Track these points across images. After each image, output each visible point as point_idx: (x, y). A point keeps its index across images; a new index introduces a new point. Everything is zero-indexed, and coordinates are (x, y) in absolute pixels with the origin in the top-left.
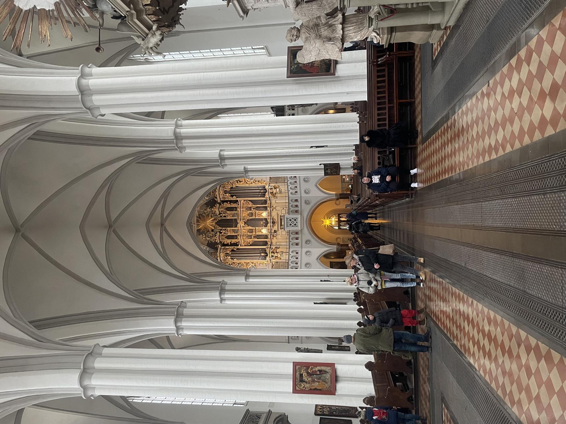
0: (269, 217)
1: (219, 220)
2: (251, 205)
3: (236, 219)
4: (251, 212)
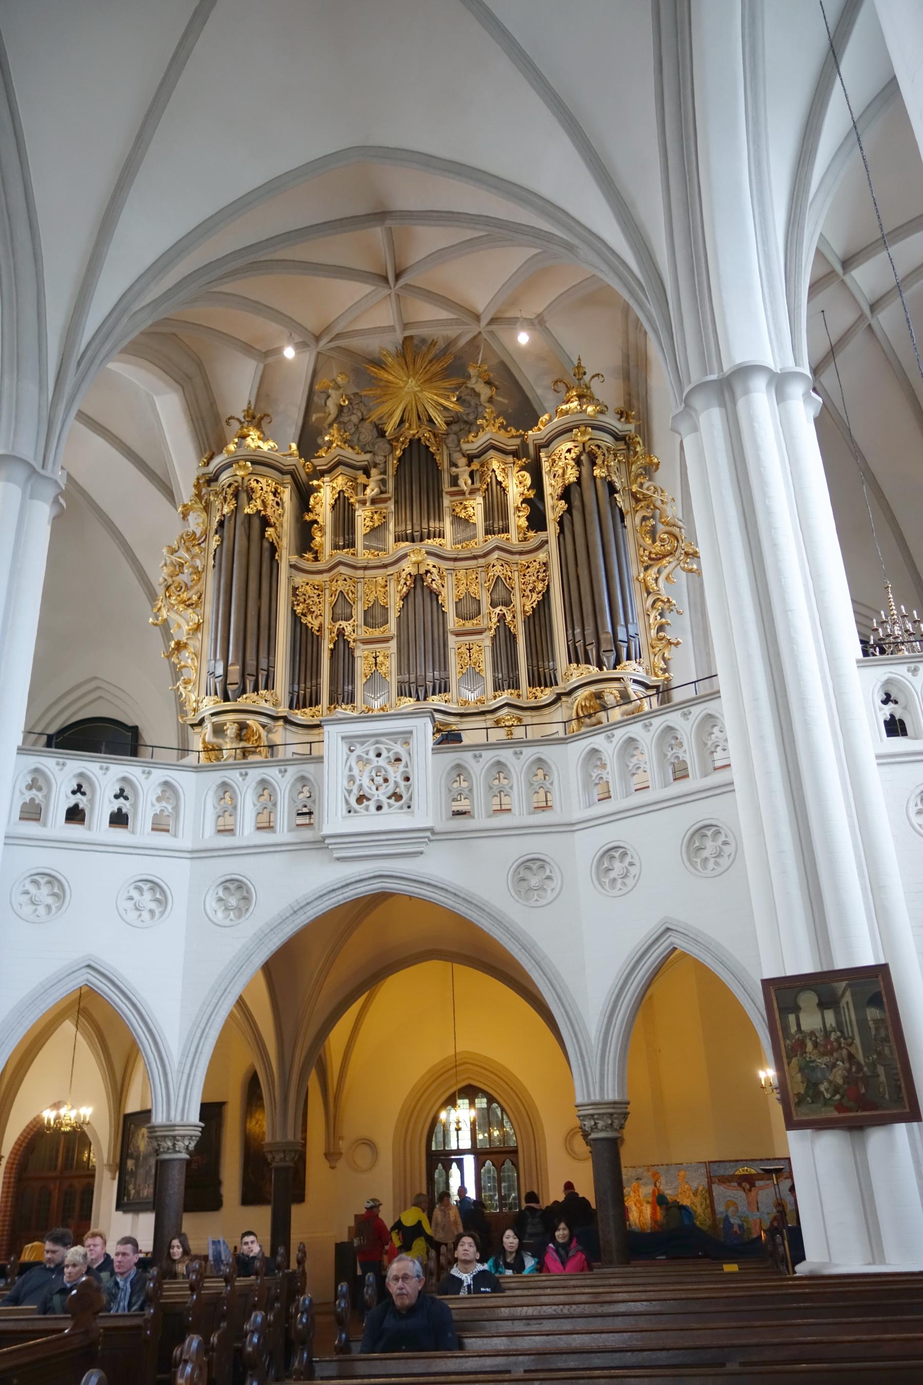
0: (453, 707)
1: (433, 454)
2: (524, 604)
4: (485, 606)
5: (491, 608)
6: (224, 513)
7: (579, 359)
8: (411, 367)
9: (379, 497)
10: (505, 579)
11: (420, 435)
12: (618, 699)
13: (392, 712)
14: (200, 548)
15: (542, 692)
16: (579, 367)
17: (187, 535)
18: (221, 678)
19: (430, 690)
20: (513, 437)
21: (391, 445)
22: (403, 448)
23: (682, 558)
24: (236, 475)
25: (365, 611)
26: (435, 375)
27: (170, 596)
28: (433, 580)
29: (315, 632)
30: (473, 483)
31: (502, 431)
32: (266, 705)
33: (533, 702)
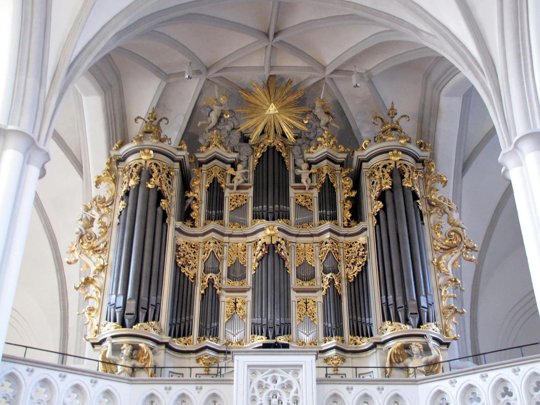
3: (286, 216)
4: (318, 272)
5: (323, 274)
6: (130, 185)
7: (393, 104)
8: (273, 96)
9: (242, 185)
10: (335, 253)
11: (275, 144)
12: (422, 350)
13: (246, 346)
14: (108, 209)
15: (360, 340)
16: (392, 109)
17: (99, 199)
18: (121, 309)
19: (277, 332)
20: (342, 152)
21: (253, 149)
22: (262, 151)
23: (464, 250)
24: (141, 159)
25: (228, 267)
26: (290, 103)
27: (82, 243)
28: (282, 249)
29: (191, 280)
30: (311, 182)
31: (335, 147)
32: (155, 333)
33: (354, 347)
